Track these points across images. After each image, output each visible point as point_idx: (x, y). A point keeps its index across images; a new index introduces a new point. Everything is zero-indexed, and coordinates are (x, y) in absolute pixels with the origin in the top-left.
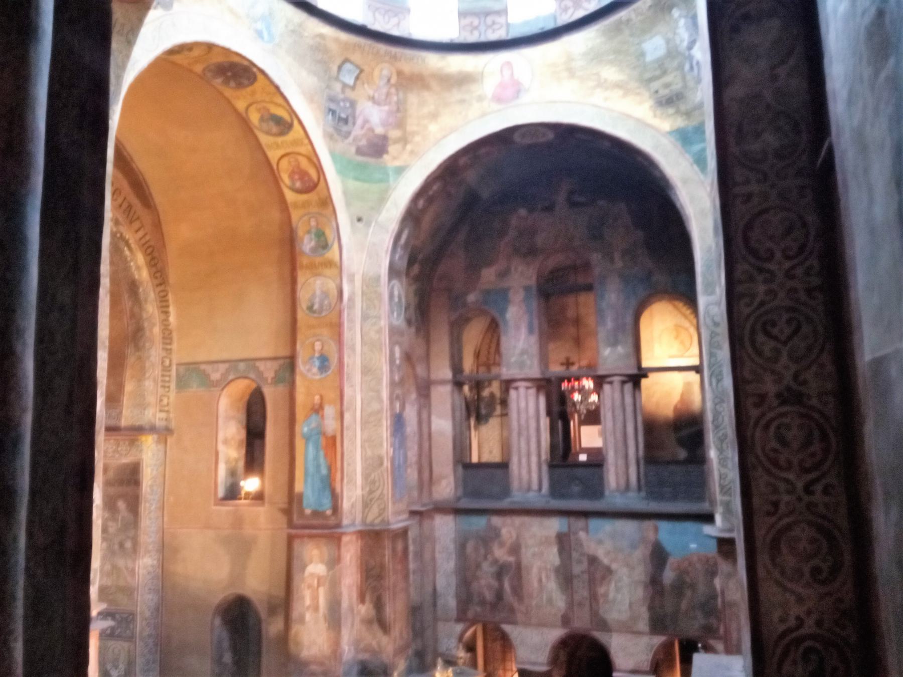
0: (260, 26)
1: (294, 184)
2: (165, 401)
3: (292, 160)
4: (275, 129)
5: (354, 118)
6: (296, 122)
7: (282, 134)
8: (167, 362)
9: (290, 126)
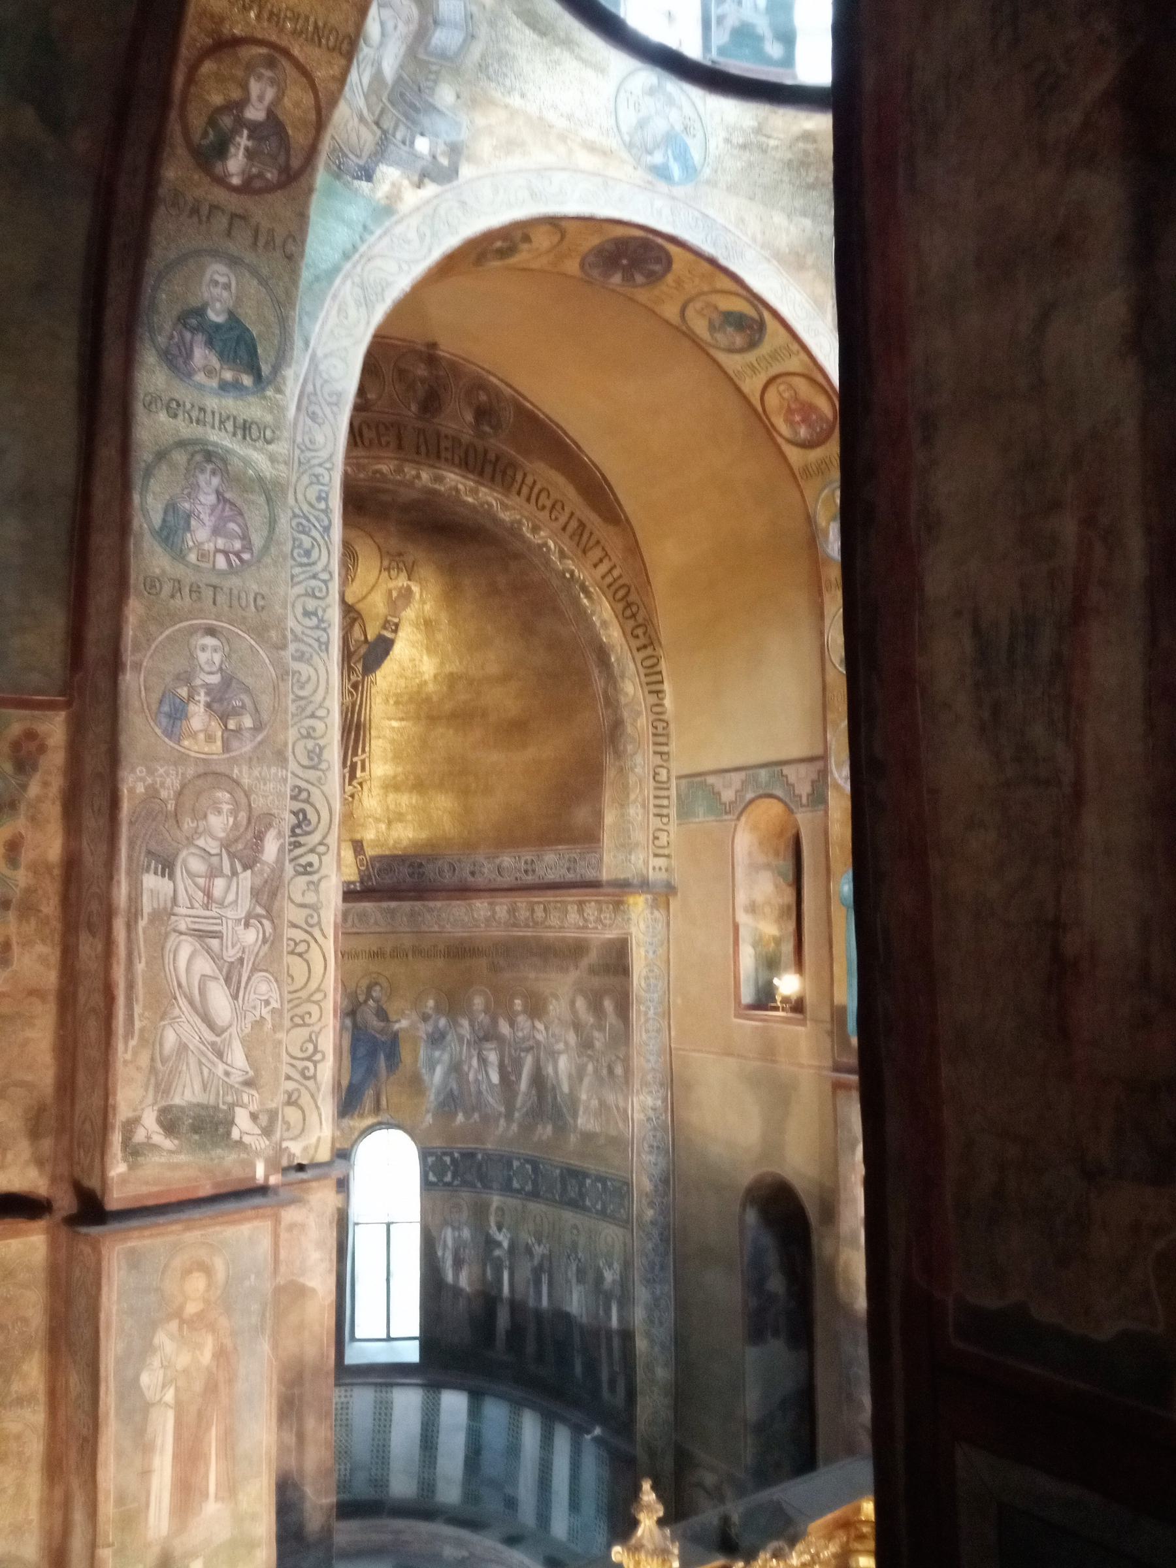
0: (658, 158)
1: (796, 433)
2: (663, 838)
3: (782, 388)
4: (739, 340)
6: (767, 315)
7: (752, 345)
8: (664, 778)
9: (762, 325)
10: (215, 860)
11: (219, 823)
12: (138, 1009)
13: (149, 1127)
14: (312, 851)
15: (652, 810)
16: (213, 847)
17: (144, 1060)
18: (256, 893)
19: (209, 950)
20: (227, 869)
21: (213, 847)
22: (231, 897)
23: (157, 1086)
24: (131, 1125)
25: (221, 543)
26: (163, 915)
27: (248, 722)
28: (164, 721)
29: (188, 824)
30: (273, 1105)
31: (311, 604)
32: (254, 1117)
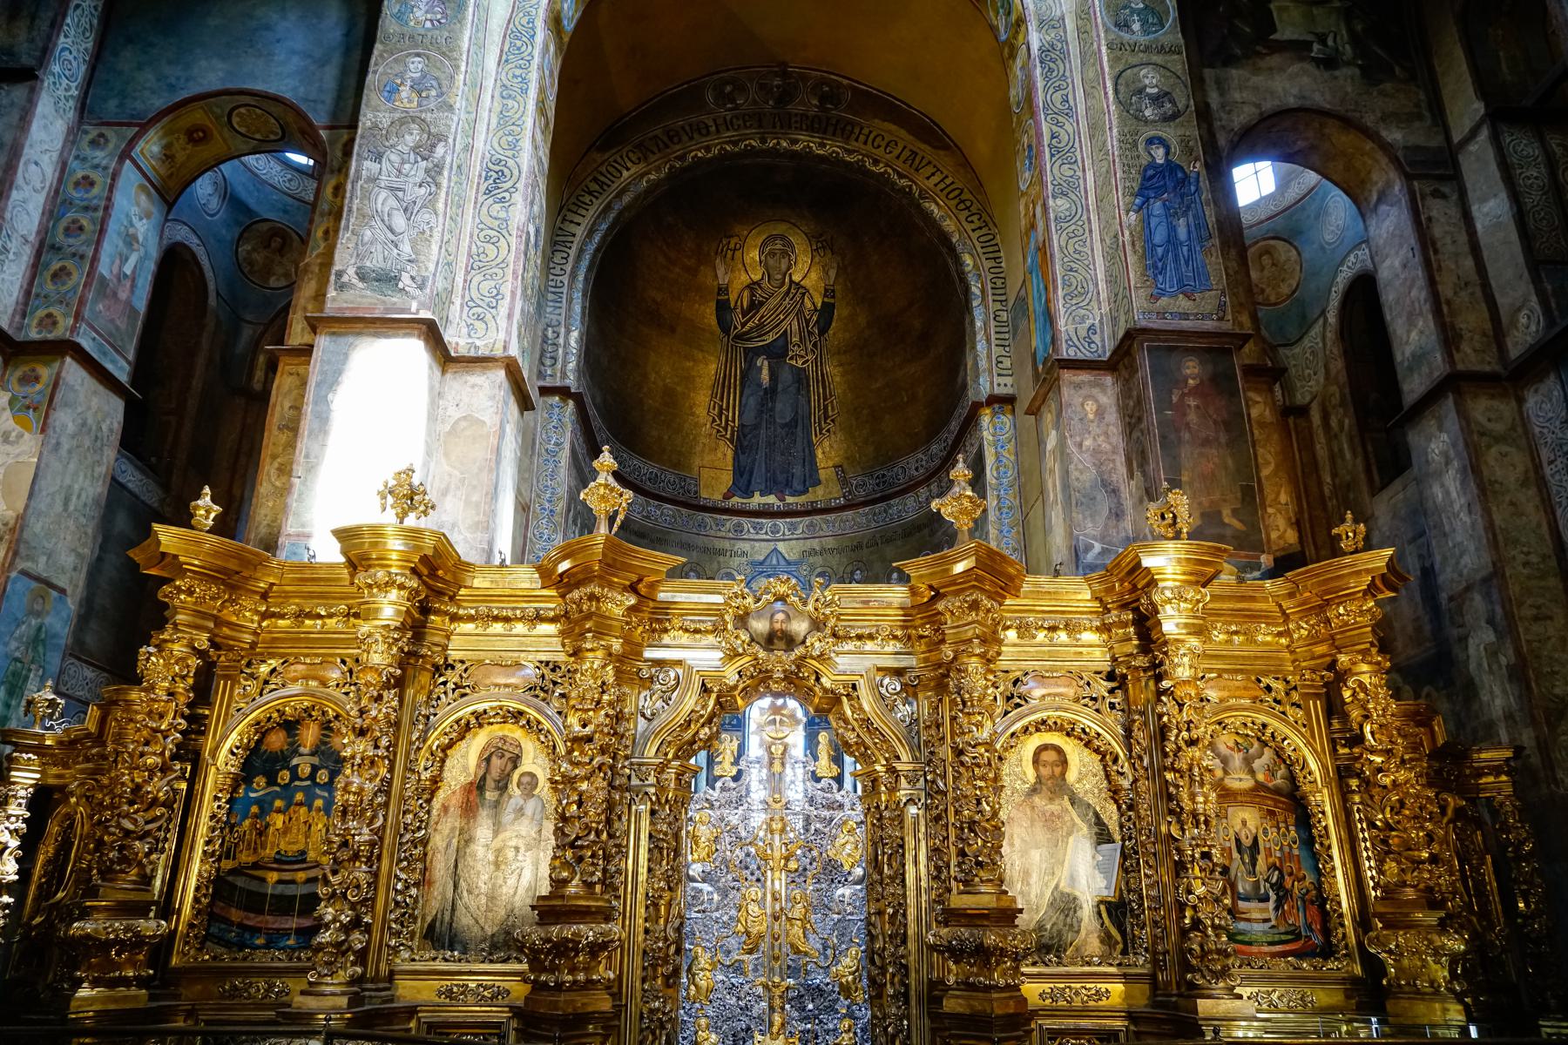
10: (406, 157)
11: (410, 140)
12: (352, 220)
13: (350, 275)
14: (506, 191)
16: (406, 149)
18: (427, 171)
19: (397, 198)
20: (412, 160)
21: (406, 149)
22: (413, 173)
23: (358, 255)
24: (339, 274)
25: (429, 16)
26: (373, 180)
27: (433, 93)
28: (386, 94)
29: (393, 140)
31: (518, 72)
32: (413, 278)
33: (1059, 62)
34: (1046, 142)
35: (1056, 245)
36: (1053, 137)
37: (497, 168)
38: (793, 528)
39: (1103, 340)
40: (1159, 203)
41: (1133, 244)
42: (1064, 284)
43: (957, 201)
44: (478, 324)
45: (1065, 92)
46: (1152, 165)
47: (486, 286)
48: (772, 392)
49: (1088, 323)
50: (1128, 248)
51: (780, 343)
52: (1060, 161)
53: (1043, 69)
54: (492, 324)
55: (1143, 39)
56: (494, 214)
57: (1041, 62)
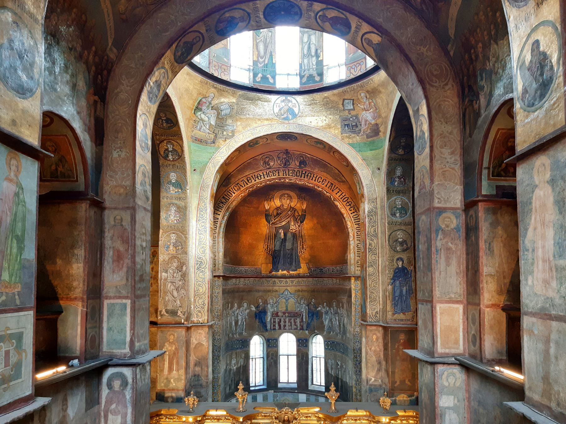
5: (360, 122)
15: (356, 255)
17: (163, 302)
30: (184, 311)
33: (374, 216)
34: (367, 247)
35: (368, 284)
36: (370, 245)
37: (200, 260)
38: (292, 282)
39: (380, 316)
40: (398, 282)
41: (389, 297)
42: (370, 298)
43: (346, 202)
44: (199, 314)
45: (375, 228)
46: (398, 268)
47: (201, 301)
48: (284, 240)
49: (376, 310)
50: (388, 297)
51: (287, 224)
52: (371, 254)
53: (368, 219)
54: (203, 314)
55: (399, 220)
56: (201, 276)
57: (368, 217)
